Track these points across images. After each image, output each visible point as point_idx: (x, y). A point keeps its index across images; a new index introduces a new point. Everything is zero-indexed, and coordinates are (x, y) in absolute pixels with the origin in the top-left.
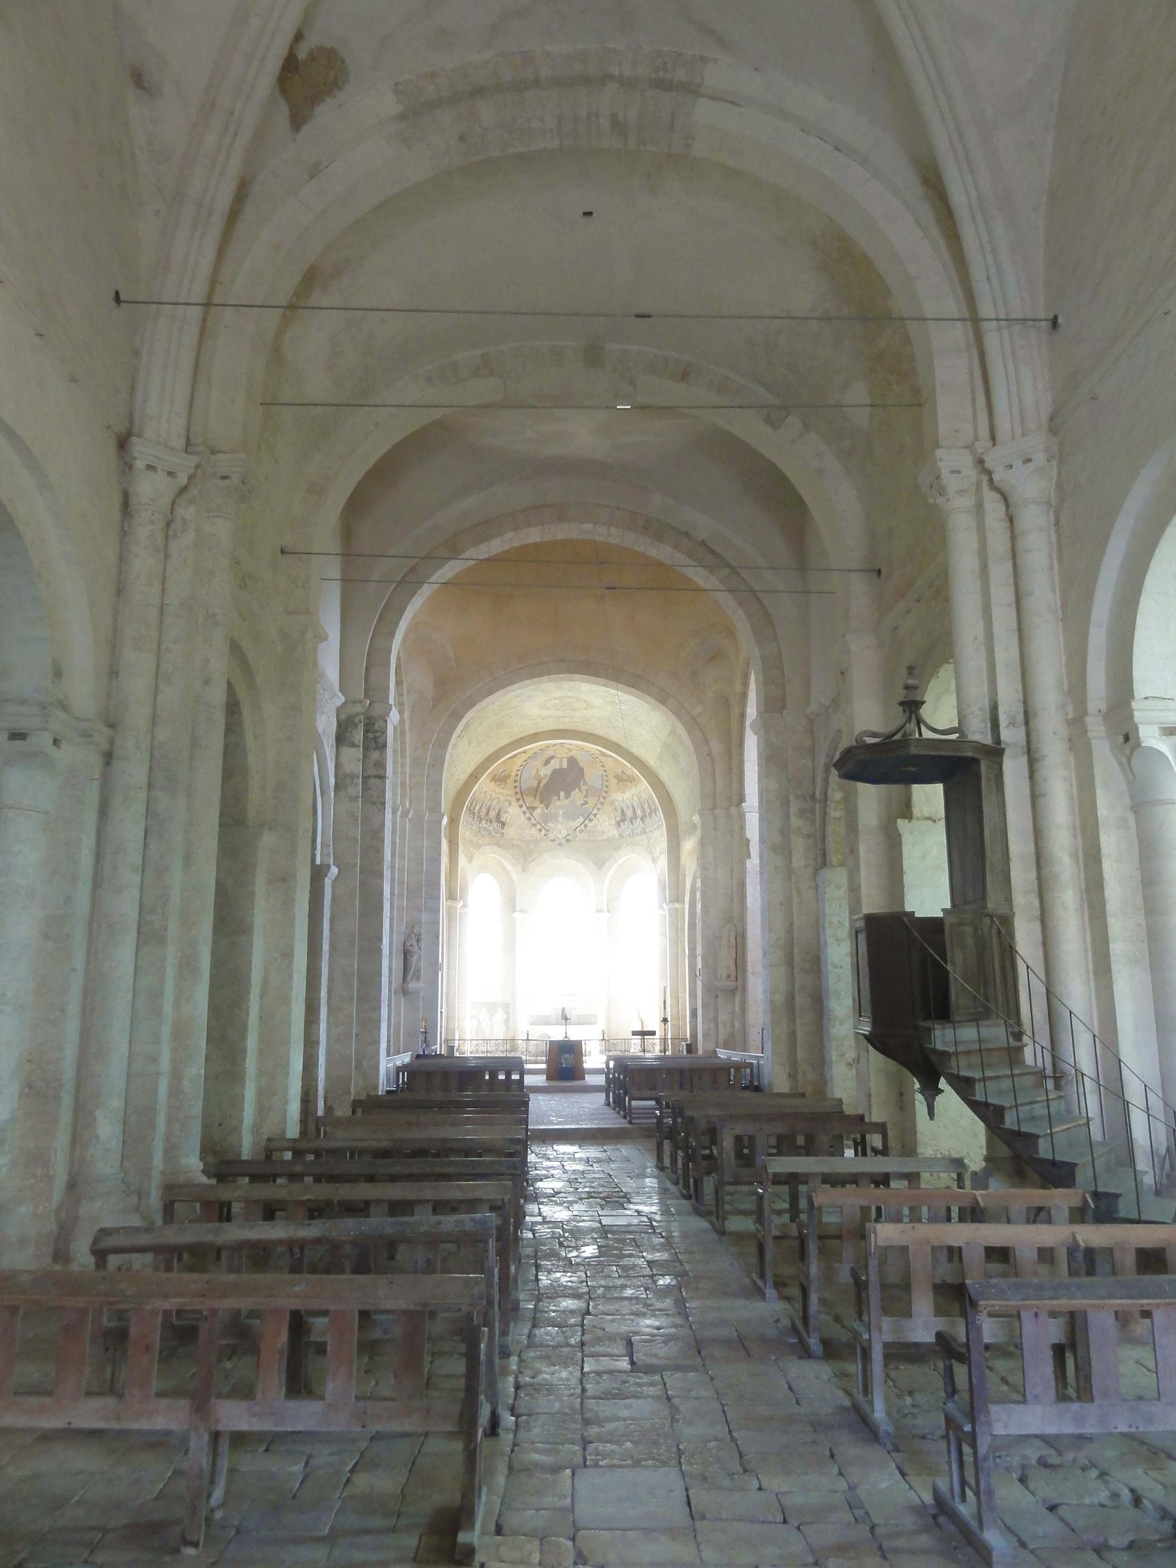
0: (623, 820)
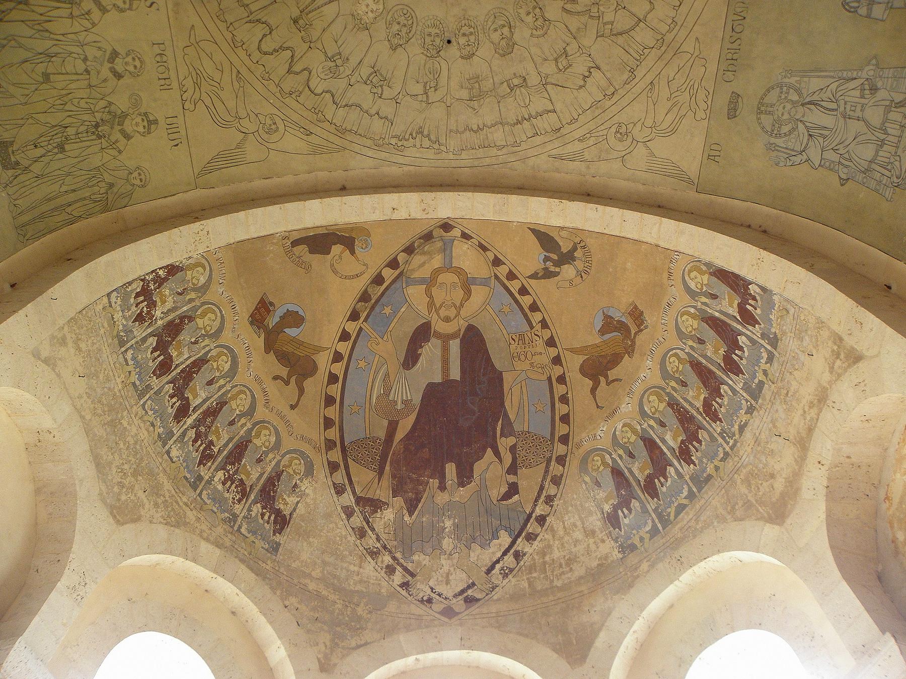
0: (624, 503)
